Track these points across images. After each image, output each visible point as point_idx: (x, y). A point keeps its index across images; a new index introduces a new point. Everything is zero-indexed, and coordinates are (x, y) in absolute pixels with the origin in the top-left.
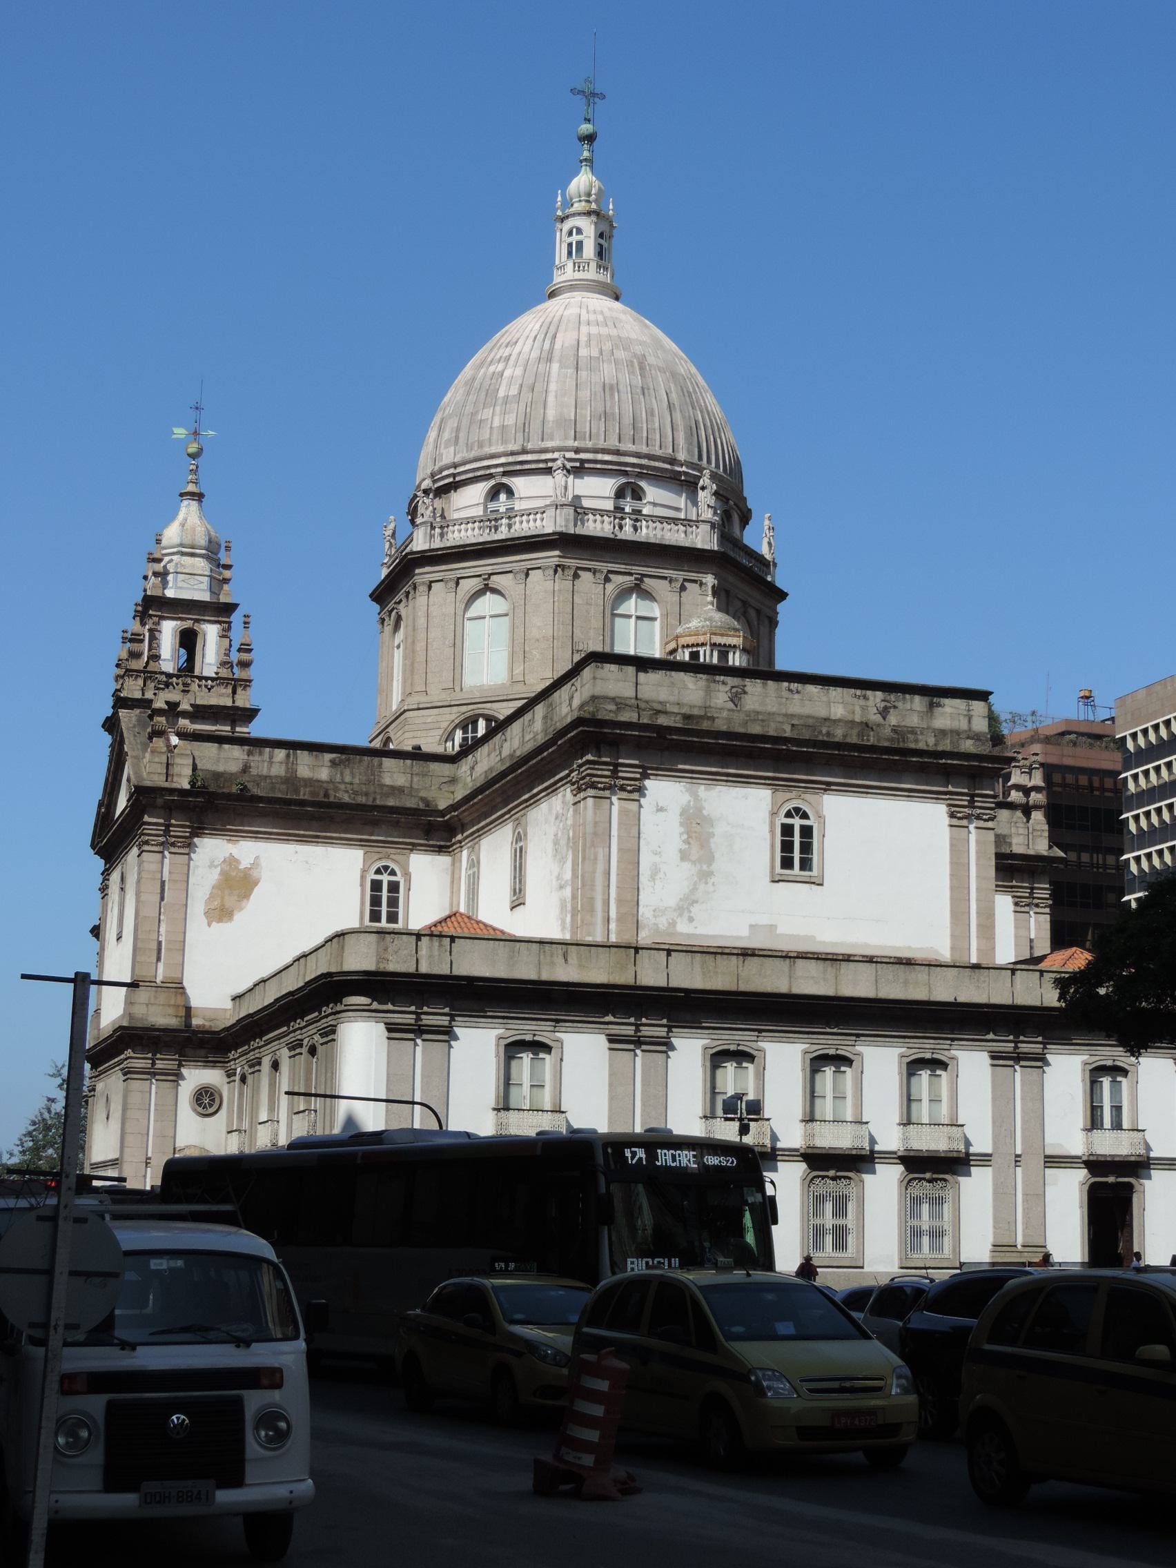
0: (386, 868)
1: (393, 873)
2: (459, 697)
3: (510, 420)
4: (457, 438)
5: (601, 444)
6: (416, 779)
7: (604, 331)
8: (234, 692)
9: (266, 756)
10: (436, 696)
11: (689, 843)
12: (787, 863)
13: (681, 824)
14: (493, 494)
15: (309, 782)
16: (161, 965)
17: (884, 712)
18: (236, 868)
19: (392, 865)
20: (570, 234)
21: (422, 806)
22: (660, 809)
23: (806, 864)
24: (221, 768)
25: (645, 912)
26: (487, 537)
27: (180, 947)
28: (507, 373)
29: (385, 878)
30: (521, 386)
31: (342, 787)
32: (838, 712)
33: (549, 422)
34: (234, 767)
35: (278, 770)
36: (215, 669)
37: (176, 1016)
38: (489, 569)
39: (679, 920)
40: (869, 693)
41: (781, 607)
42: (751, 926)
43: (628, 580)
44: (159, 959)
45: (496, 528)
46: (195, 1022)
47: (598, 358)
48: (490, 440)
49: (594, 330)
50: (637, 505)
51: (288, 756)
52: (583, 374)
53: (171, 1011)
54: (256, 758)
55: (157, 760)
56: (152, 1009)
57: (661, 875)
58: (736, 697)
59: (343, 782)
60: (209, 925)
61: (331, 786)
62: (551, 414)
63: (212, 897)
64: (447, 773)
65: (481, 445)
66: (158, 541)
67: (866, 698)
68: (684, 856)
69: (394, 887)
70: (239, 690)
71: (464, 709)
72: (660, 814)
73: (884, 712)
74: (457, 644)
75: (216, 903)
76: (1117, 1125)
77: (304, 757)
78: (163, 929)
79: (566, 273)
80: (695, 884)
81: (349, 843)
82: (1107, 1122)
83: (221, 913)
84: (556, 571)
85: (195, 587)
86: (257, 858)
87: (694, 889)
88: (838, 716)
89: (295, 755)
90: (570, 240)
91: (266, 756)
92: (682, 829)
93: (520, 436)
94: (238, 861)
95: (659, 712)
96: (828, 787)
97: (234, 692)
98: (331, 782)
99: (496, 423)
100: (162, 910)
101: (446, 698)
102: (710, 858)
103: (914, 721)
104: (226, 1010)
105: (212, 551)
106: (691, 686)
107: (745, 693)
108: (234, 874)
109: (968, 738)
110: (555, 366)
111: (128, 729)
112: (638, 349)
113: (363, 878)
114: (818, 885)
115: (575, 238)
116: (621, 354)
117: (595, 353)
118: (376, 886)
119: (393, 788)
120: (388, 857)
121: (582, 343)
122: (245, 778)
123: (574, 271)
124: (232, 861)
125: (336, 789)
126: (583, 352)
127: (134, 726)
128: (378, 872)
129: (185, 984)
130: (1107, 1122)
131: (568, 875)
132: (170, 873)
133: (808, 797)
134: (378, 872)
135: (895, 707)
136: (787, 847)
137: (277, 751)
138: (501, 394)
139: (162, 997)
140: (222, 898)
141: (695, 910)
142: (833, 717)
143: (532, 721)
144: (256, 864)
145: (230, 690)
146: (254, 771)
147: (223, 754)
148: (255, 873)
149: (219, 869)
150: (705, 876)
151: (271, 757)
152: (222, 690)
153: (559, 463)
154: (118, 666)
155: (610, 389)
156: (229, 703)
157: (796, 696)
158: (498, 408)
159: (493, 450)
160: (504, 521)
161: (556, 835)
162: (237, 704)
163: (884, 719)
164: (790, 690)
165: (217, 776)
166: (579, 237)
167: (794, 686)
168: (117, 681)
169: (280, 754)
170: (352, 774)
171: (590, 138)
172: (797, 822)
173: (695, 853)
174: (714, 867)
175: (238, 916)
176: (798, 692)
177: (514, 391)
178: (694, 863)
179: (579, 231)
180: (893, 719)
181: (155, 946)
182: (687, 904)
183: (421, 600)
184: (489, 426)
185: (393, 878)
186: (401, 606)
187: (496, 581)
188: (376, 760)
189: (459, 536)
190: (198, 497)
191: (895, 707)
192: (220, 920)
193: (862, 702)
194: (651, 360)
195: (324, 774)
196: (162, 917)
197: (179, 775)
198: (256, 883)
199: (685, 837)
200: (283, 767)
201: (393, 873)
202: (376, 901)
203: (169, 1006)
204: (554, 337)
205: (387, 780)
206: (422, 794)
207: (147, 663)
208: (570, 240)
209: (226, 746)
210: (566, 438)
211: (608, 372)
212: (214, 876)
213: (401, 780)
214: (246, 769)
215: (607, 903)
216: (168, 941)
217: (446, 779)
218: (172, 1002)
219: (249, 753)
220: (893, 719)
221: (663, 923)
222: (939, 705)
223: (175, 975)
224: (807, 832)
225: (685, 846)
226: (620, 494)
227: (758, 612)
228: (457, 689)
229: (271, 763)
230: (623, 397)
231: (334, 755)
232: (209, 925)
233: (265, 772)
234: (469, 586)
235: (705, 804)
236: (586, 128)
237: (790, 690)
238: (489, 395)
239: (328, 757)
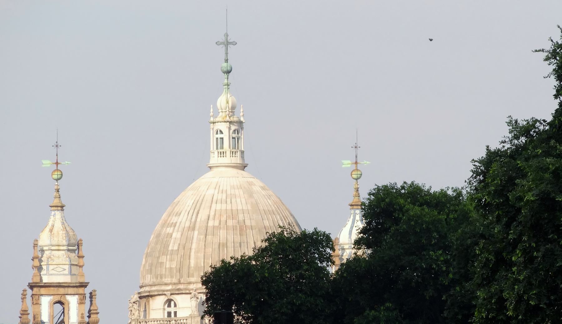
3: (174, 266)
4: (151, 270)
14: (169, 302)
28: (174, 236)
30: (179, 244)
33: (191, 267)
47: (218, 227)
48: (165, 275)
49: (219, 207)
52: (209, 237)
79: (215, 159)
85: (61, 273)
93: (178, 274)
99: (168, 266)
115: (219, 136)
116: (230, 223)
117: (217, 224)
121: (211, 217)
123: (218, 157)
126: (211, 223)
138: (170, 248)
158: (168, 257)
166: (221, 136)
177: (176, 248)
179: (221, 132)
184: (164, 267)
190: (62, 207)
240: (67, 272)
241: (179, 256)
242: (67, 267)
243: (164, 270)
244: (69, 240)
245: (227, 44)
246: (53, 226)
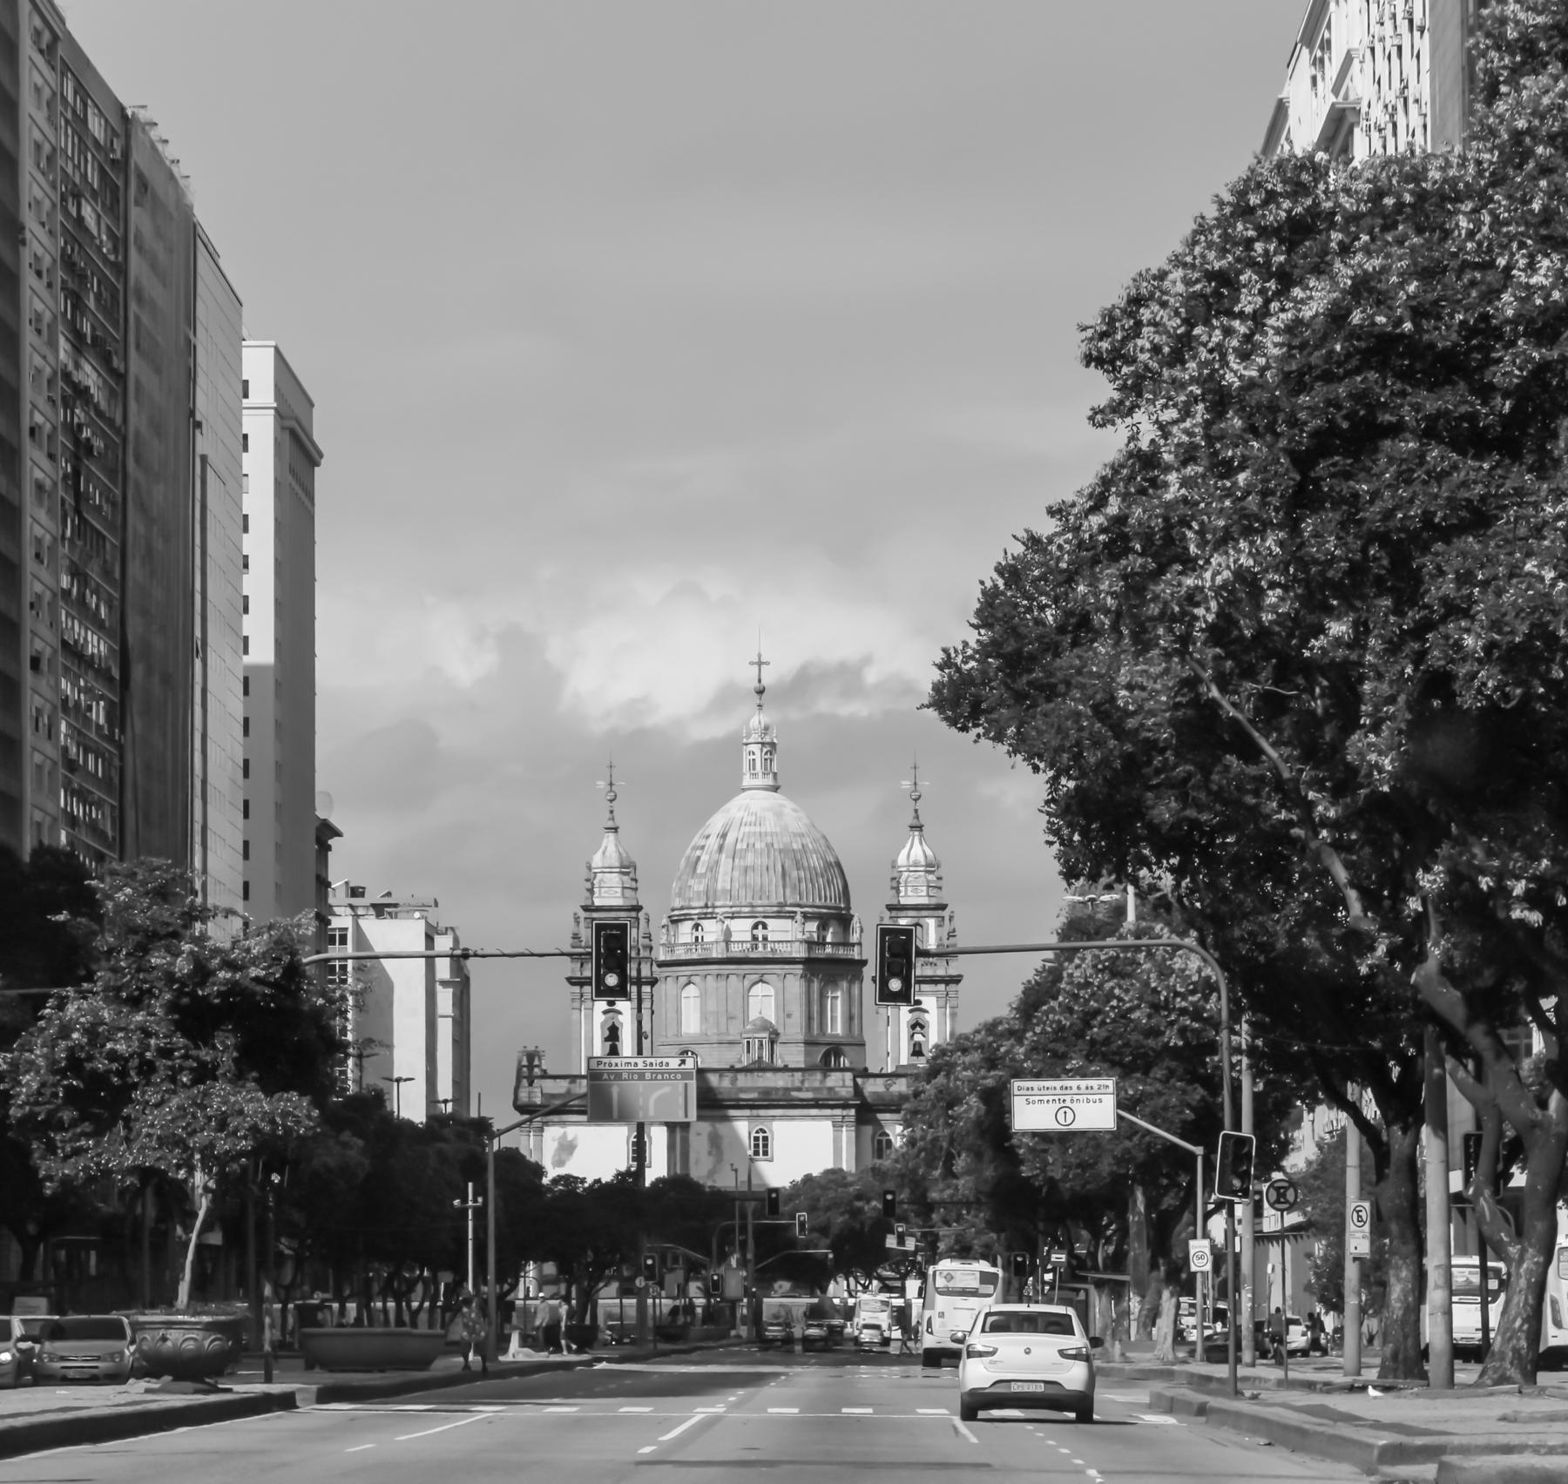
2: (679, 1040)
3: (702, 888)
7: (753, 829)
14: (696, 927)
22: (699, 1134)
23: (765, 1153)
43: (756, 977)
49: (747, 829)
50: (765, 932)
52: (737, 860)
58: (734, 1081)
62: (719, 887)
65: (690, 900)
66: (590, 868)
68: (710, 1153)
79: (747, 781)
105: (627, 868)
110: (724, 855)
112: (769, 839)
115: (752, 757)
126: (739, 847)
172: (761, 1135)
182: (712, 1173)
189: (681, 954)
190: (615, 830)
211: (750, 859)
212: (555, 1145)
224: (765, 1139)
226: (755, 927)
234: (683, 980)
240: (619, 894)
242: (619, 890)
244: (622, 862)
245: (760, 664)
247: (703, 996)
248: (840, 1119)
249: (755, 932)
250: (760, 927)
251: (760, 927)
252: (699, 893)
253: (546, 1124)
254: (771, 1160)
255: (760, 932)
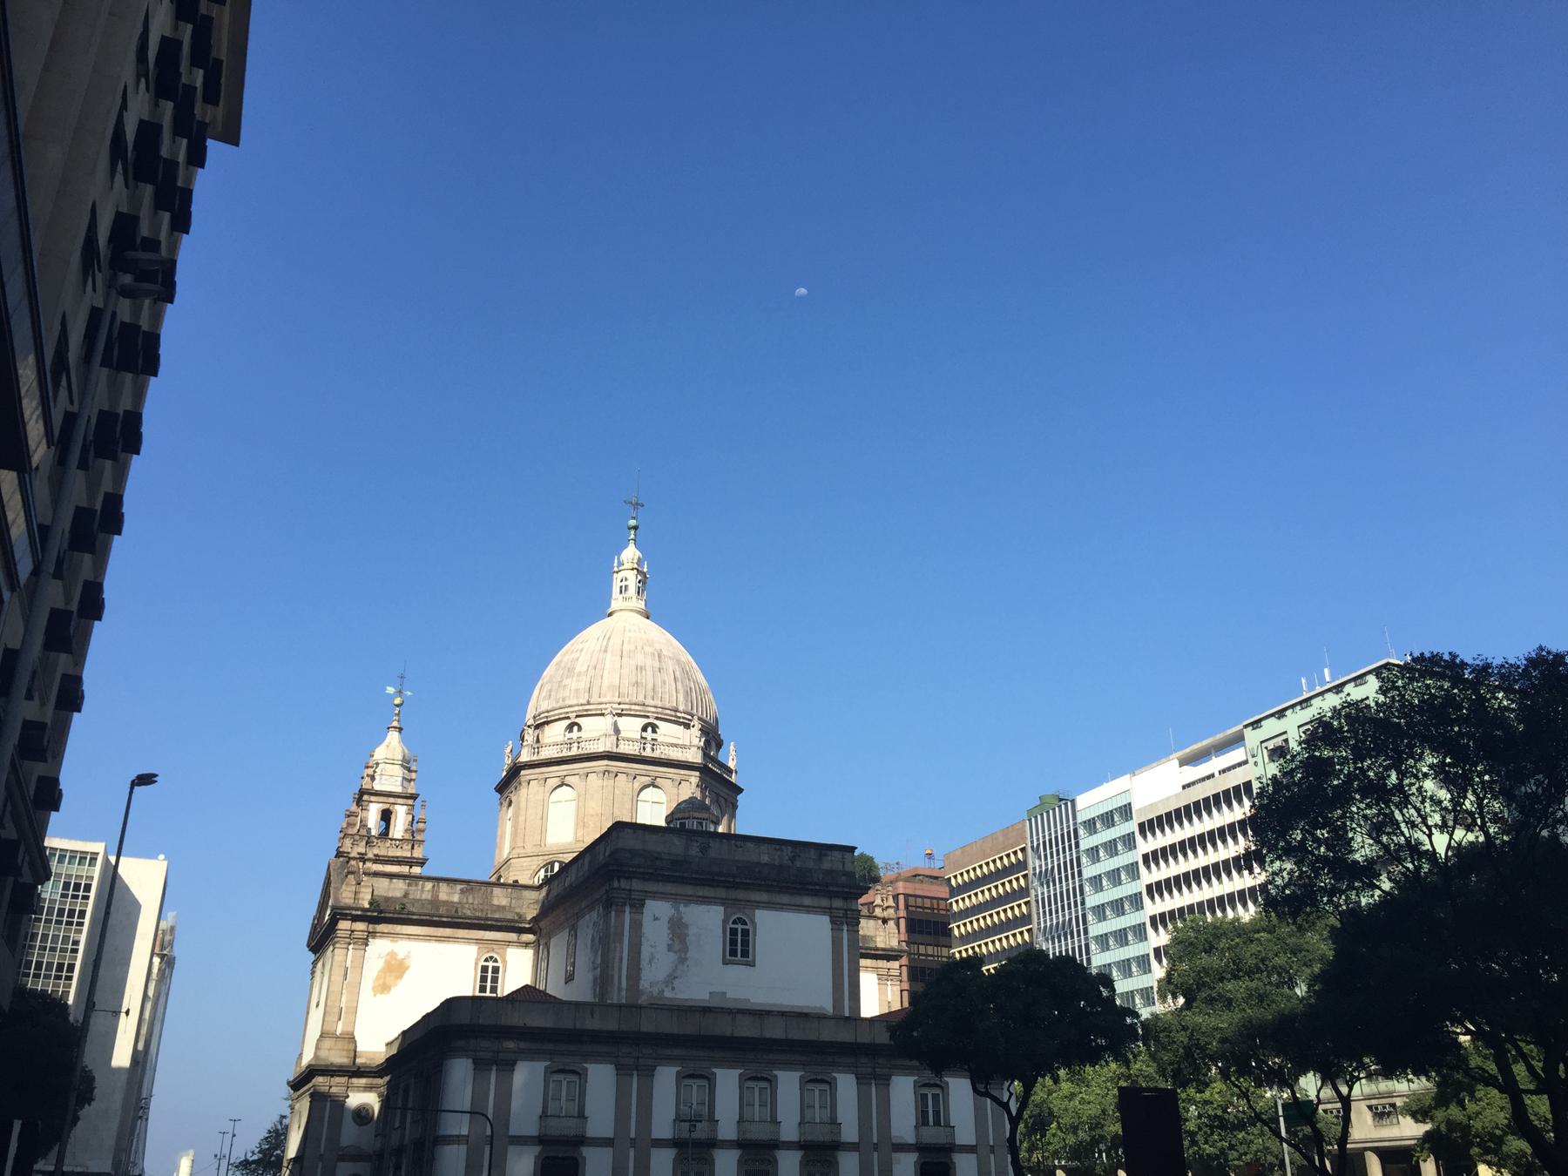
0: (491, 958)
1: (496, 961)
2: (544, 850)
4: (550, 695)
5: (634, 700)
6: (513, 901)
8: (413, 848)
9: (420, 887)
10: (530, 850)
11: (673, 940)
12: (733, 953)
13: (669, 928)
14: (570, 728)
15: (446, 903)
16: (340, 1023)
17: (793, 859)
18: (395, 959)
19: (495, 956)
20: (622, 581)
21: (516, 918)
22: (656, 919)
23: (745, 954)
24: (390, 895)
25: (644, 984)
26: (566, 753)
27: (354, 1011)
29: (491, 964)
30: (589, 666)
31: (467, 906)
32: (765, 859)
34: (398, 894)
35: (427, 896)
36: (402, 834)
37: (348, 1057)
38: (565, 773)
39: (666, 989)
40: (784, 847)
41: (739, 797)
42: (710, 993)
43: (647, 780)
44: (340, 1019)
45: (570, 748)
46: (359, 1061)
50: (654, 736)
51: (434, 886)
52: (625, 659)
53: (345, 1053)
54: (414, 888)
55: (348, 889)
56: (332, 1052)
57: (655, 960)
58: (704, 849)
59: (467, 903)
60: (375, 995)
61: (459, 906)
62: (606, 683)
63: (378, 978)
64: (533, 897)
65: (564, 700)
67: (781, 850)
68: (670, 948)
69: (496, 970)
70: (416, 847)
71: (546, 857)
72: (657, 922)
73: (793, 859)
74: (543, 818)
75: (381, 982)
76: (937, 1123)
77: (443, 887)
78: (344, 999)
79: (617, 602)
80: (676, 966)
81: (468, 940)
82: (931, 1123)
83: (383, 988)
84: (604, 774)
86: (409, 952)
87: (675, 970)
88: (765, 861)
89: (438, 885)
90: (622, 584)
91: (420, 887)
92: (669, 932)
93: (587, 695)
94: (397, 955)
95: (657, 858)
96: (759, 905)
97: (413, 848)
98: (460, 903)
100: (344, 986)
101: (536, 850)
102: (686, 950)
103: (811, 864)
104: (381, 1053)
105: (406, 764)
106: (677, 843)
107: (709, 847)
108: (393, 962)
109: (844, 875)
110: (609, 655)
111: (334, 870)
112: (658, 647)
113: (476, 964)
114: (750, 966)
115: (624, 583)
116: (648, 649)
117: (633, 648)
118: (484, 969)
119: (499, 906)
120: (493, 950)
122: (405, 901)
124: (392, 954)
125: (463, 908)
127: (339, 868)
128: (486, 960)
129: (355, 1034)
130: (931, 1123)
131: (599, 961)
132: (352, 962)
133: (746, 911)
134: (486, 960)
135: (799, 856)
136: (733, 942)
137: (427, 883)
138: (577, 671)
139: (340, 1044)
140: (385, 978)
141: (676, 983)
142: (762, 862)
143: (583, 864)
144: (408, 956)
145: (410, 847)
146: (411, 897)
147: (392, 886)
148: (407, 962)
149: (383, 960)
150: (682, 961)
151: (423, 887)
152: (405, 847)
153: (609, 711)
154: (341, 832)
155: (640, 668)
156: (409, 855)
157: (741, 849)
158: (575, 679)
159: (571, 703)
160: (576, 744)
161: (593, 936)
162: (414, 855)
163: (793, 863)
164: (736, 846)
165: (387, 899)
167: (739, 843)
168: (339, 841)
169: (429, 885)
170: (474, 898)
171: (635, 528)
172: (740, 927)
173: (676, 947)
174: (688, 955)
175: (393, 990)
176: (741, 847)
178: (676, 952)
180: (798, 864)
181: (337, 1010)
182: (671, 979)
183: (523, 791)
185: (495, 964)
186: (512, 795)
187: (568, 780)
188: (489, 889)
189: (547, 753)
191: (799, 856)
192: (382, 992)
193: (779, 853)
194: (665, 652)
195: (456, 898)
196: (344, 991)
197: (363, 899)
198: (407, 968)
199: (671, 936)
200: (430, 894)
201: (496, 961)
202: (483, 979)
203: (344, 1050)
204: (609, 638)
205: (495, 902)
206: (517, 910)
207: (359, 830)
208: (622, 584)
209: (394, 881)
210: (613, 696)
211: (640, 659)
212: (380, 964)
213: (504, 902)
214: (406, 895)
215: (620, 977)
216: (347, 1007)
217: (532, 901)
218: (346, 1048)
219: (409, 885)
220: (798, 864)
221: (656, 991)
222: (826, 855)
223: (349, 1029)
224: (745, 933)
225: (671, 942)
226: (644, 729)
227: (726, 800)
228: (543, 845)
229: (422, 891)
230: (648, 673)
231: (463, 886)
232: (375, 995)
233: (418, 897)
234: (553, 782)
235: (683, 916)
236: (632, 522)
237: (736, 846)
238: (570, 671)
239: (459, 887)
240: (399, 783)
241: (589, 677)
242: (400, 779)
243: (568, 691)
244: (404, 757)
246: (390, 743)
247: (581, 800)
248: (841, 913)
249: (644, 734)
250: (650, 729)
251: (650, 729)
252: (577, 691)
253: (373, 934)
254: (752, 964)
255: (649, 734)
